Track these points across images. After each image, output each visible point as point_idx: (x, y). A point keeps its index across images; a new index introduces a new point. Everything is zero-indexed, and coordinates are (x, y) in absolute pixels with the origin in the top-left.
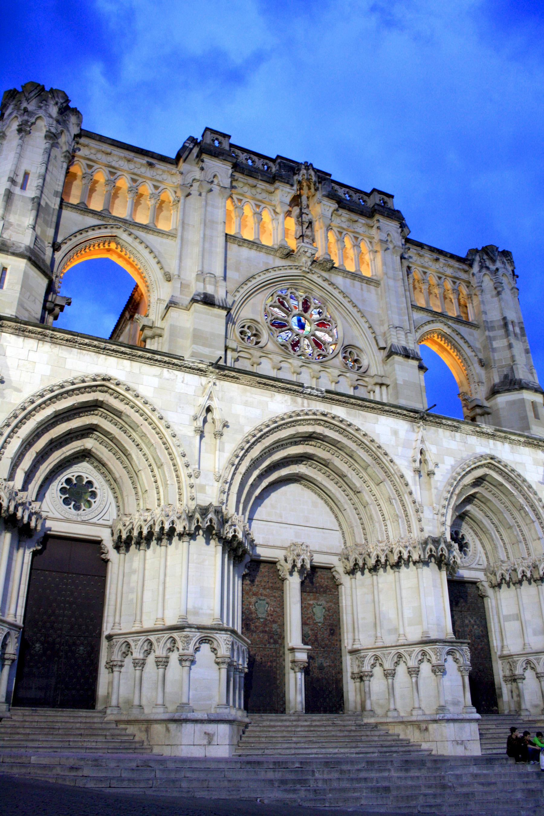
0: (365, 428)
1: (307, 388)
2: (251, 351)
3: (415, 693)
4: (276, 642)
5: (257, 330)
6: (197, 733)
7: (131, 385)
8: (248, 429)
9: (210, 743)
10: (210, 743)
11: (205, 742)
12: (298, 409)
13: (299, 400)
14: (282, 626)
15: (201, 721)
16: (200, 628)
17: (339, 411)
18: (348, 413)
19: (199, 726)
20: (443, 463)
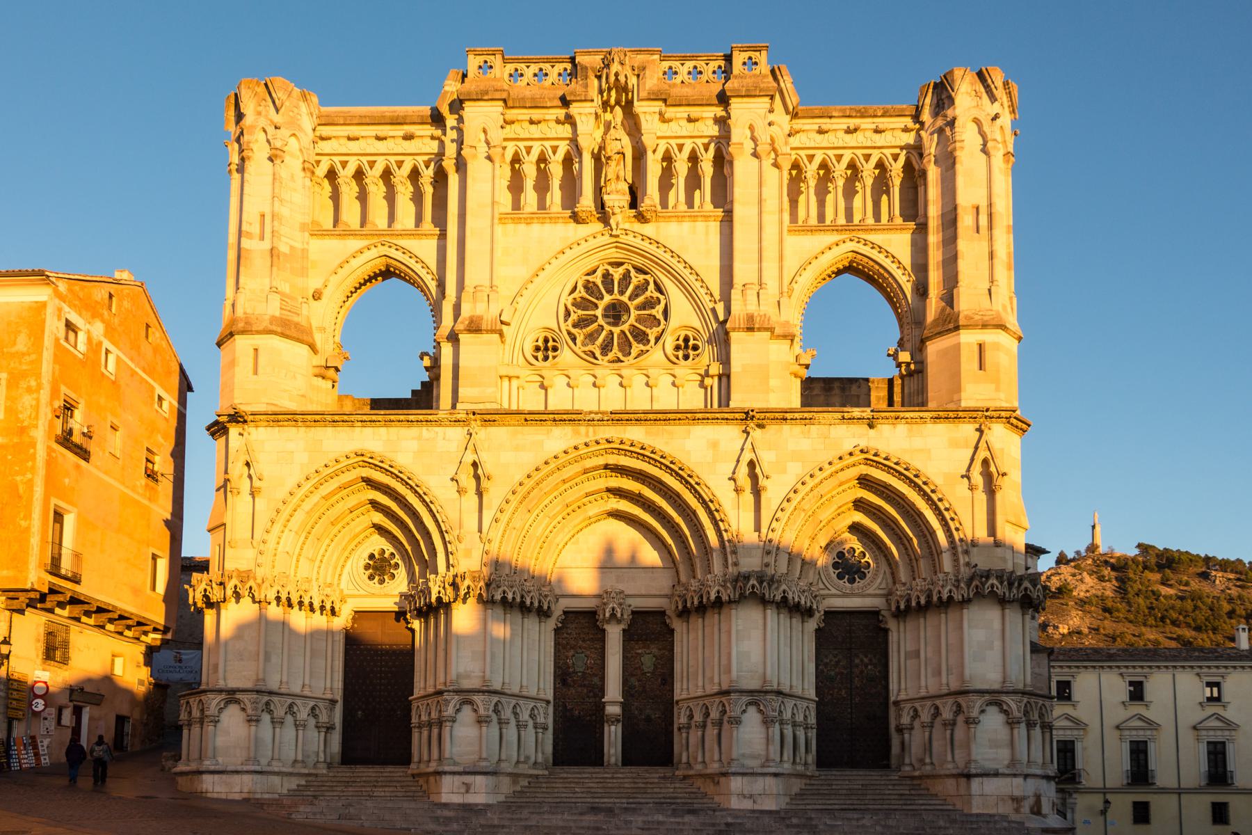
0: (667, 450)
1: (591, 412)
2: (543, 373)
3: (716, 747)
4: (595, 696)
5: (554, 340)
6: (456, 783)
7: (389, 455)
8: (519, 477)
9: (467, 792)
10: (467, 792)
11: (463, 790)
12: (580, 441)
13: (583, 429)
14: (603, 679)
15: (459, 773)
16: (457, 692)
17: (635, 434)
18: (647, 433)
19: (457, 778)
20: (784, 471)
